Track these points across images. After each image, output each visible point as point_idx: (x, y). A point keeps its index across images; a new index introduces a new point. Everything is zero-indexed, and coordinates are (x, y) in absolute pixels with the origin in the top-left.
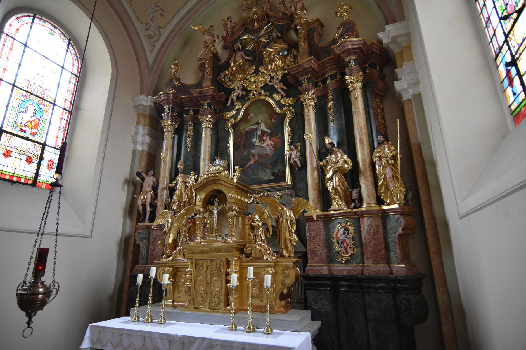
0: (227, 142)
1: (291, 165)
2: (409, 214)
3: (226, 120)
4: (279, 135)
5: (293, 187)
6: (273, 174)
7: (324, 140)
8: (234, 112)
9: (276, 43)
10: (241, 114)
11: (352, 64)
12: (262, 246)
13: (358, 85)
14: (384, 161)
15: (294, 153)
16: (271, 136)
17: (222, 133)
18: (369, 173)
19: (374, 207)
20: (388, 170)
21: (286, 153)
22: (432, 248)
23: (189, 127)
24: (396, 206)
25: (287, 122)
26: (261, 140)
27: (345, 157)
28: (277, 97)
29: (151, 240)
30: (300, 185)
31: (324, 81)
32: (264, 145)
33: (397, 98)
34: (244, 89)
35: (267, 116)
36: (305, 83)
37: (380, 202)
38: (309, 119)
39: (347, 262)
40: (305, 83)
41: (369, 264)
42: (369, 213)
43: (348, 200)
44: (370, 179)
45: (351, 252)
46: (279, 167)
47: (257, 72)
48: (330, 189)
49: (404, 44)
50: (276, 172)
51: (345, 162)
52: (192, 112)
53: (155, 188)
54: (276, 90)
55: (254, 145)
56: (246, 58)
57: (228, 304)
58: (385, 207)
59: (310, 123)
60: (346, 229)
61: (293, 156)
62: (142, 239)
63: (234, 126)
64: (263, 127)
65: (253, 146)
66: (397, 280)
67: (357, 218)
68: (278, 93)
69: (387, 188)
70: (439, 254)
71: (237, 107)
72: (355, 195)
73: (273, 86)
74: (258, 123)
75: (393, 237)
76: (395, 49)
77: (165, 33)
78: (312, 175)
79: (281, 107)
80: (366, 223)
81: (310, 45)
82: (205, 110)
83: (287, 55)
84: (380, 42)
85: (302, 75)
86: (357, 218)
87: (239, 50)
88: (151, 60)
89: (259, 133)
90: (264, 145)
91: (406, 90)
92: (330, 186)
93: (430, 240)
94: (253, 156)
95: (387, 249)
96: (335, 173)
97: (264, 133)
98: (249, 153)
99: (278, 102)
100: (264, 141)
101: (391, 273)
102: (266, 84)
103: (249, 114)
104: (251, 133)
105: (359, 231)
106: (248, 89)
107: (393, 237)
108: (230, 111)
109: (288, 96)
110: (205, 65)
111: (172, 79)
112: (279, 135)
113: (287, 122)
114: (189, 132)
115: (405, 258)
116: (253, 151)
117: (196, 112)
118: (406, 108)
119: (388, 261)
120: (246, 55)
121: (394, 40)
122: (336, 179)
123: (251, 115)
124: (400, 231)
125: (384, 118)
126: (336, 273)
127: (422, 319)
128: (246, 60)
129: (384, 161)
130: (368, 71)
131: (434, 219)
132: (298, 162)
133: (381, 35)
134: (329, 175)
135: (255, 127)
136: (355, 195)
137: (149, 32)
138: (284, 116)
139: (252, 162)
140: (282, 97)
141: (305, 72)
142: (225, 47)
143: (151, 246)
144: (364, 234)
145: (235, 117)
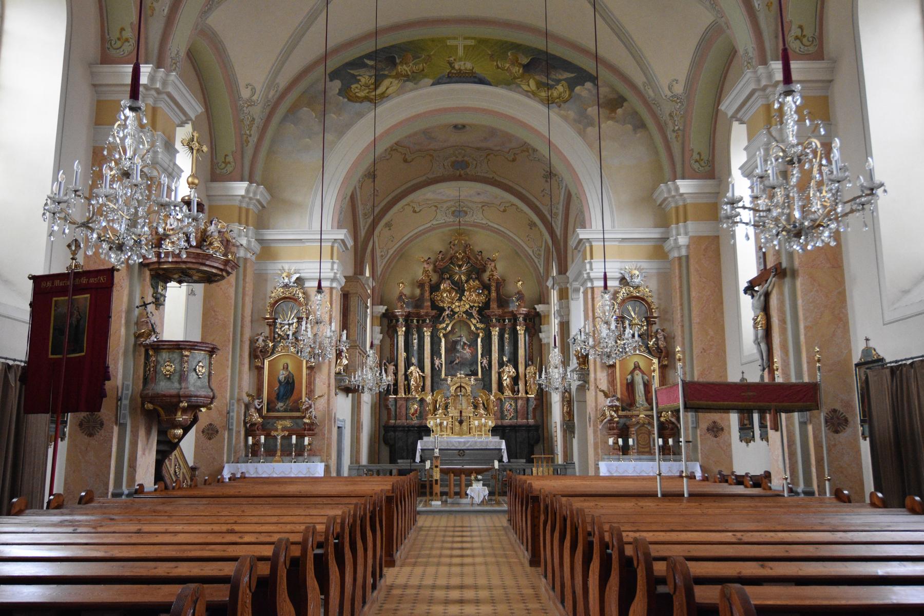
0: (440, 345)
1: (482, 367)
2: (538, 399)
3: (438, 330)
4: (475, 347)
5: (483, 379)
6: (471, 371)
7: (503, 358)
8: (444, 325)
9: (474, 281)
10: (449, 328)
11: (521, 319)
12: (482, 411)
13: (523, 332)
14: (530, 374)
15: (485, 361)
16: (469, 346)
17: (435, 338)
18: (523, 380)
19: (524, 395)
20: (532, 380)
21: (479, 360)
22: (545, 414)
23: (415, 333)
24: (533, 396)
25: (479, 340)
26: (463, 348)
27: (514, 370)
28: (474, 321)
29: (398, 406)
30: (487, 379)
31: (504, 321)
32: (465, 352)
33: (540, 340)
34: (452, 310)
35: (467, 333)
36: (494, 320)
37: (527, 393)
38: (495, 344)
39: (510, 419)
40: (494, 320)
41: (519, 420)
42: (522, 398)
43: (513, 391)
44: (524, 382)
45: (512, 415)
46: (475, 366)
47: (460, 299)
48: (505, 385)
49: (546, 314)
50: (473, 369)
51: (514, 372)
52: (415, 321)
53: (396, 374)
54: (473, 316)
55: (458, 351)
56: (453, 286)
57: (470, 433)
58: (529, 396)
59: (495, 346)
60: (511, 405)
61: (484, 362)
62: (392, 405)
63: (444, 335)
64: (464, 340)
65: (458, 351)
66: (530, 426)
67: (516, 400)
68: (475, 319)
69: (530, 387)
70: (547, 417)
71: (446, 322)
72: (516, 389)
73: (472, 313)
74: (460, 336)
75: (531, 409)
76: (542, 314)
77: (391, 252)
78: (495, 376)
79: (477, 329)
80: (520, 402)
81: (497, 294)
82: (428, 324)
83: (481, 293)
84: (535, 309)
85: (493, 316)
86: (516, 400)
87: (448, 279)
88: (379, 273)
89: (462, 343)
90: (465, 352)
91: (544, 338)
92: (505, 383)
93: (545, 410)
94: (458, 358)
95: (528, 414)
96: (508, 377)
97: (465, 344)
98: (455, 356)
99: (475, 325)
100: (465, 349)
101: (528, 424)
102: (467, 310)
103: (455, 329)
104: (455, 343)
105: (516, 406)
106: (454, 310)
107: (531, 409)
108: (441, 324)
109: (481, 322)
110: (424, 286)
111: (401, 296)
112: (475, 347)
113: (479, 340)
114: (414, 336)
115: (534, 417)
116: (458, 355)
117: (418, 321)
118: (543, 347)
119: (527, 419)
120: (452, 282)
121: (542, 311)
122: (508, 380)
123: (457, 330)
124: (534, 406)
125: (532, 349)
126: (504, 424)
127: (537, 442)
128: (452, 288)
129: (530, 374)
130: (528, 321)
131: (547, 401)
132: (487, 367)
133: (536, 306)
134: (505, 378)
135: (459, 339)
136: (516, 389)
137: (383, 253)
138: (478, 335)
139: (457, 361)
140: (477, 322)
141: (495, 315)
142: (435, 271)
143: (398, 410)
144: (519, 407)
145: (445, 329)
